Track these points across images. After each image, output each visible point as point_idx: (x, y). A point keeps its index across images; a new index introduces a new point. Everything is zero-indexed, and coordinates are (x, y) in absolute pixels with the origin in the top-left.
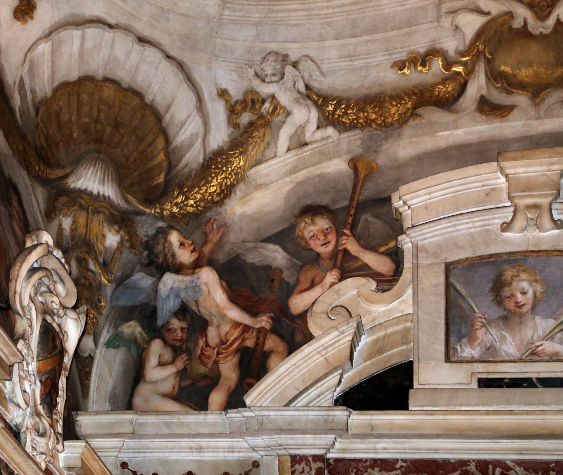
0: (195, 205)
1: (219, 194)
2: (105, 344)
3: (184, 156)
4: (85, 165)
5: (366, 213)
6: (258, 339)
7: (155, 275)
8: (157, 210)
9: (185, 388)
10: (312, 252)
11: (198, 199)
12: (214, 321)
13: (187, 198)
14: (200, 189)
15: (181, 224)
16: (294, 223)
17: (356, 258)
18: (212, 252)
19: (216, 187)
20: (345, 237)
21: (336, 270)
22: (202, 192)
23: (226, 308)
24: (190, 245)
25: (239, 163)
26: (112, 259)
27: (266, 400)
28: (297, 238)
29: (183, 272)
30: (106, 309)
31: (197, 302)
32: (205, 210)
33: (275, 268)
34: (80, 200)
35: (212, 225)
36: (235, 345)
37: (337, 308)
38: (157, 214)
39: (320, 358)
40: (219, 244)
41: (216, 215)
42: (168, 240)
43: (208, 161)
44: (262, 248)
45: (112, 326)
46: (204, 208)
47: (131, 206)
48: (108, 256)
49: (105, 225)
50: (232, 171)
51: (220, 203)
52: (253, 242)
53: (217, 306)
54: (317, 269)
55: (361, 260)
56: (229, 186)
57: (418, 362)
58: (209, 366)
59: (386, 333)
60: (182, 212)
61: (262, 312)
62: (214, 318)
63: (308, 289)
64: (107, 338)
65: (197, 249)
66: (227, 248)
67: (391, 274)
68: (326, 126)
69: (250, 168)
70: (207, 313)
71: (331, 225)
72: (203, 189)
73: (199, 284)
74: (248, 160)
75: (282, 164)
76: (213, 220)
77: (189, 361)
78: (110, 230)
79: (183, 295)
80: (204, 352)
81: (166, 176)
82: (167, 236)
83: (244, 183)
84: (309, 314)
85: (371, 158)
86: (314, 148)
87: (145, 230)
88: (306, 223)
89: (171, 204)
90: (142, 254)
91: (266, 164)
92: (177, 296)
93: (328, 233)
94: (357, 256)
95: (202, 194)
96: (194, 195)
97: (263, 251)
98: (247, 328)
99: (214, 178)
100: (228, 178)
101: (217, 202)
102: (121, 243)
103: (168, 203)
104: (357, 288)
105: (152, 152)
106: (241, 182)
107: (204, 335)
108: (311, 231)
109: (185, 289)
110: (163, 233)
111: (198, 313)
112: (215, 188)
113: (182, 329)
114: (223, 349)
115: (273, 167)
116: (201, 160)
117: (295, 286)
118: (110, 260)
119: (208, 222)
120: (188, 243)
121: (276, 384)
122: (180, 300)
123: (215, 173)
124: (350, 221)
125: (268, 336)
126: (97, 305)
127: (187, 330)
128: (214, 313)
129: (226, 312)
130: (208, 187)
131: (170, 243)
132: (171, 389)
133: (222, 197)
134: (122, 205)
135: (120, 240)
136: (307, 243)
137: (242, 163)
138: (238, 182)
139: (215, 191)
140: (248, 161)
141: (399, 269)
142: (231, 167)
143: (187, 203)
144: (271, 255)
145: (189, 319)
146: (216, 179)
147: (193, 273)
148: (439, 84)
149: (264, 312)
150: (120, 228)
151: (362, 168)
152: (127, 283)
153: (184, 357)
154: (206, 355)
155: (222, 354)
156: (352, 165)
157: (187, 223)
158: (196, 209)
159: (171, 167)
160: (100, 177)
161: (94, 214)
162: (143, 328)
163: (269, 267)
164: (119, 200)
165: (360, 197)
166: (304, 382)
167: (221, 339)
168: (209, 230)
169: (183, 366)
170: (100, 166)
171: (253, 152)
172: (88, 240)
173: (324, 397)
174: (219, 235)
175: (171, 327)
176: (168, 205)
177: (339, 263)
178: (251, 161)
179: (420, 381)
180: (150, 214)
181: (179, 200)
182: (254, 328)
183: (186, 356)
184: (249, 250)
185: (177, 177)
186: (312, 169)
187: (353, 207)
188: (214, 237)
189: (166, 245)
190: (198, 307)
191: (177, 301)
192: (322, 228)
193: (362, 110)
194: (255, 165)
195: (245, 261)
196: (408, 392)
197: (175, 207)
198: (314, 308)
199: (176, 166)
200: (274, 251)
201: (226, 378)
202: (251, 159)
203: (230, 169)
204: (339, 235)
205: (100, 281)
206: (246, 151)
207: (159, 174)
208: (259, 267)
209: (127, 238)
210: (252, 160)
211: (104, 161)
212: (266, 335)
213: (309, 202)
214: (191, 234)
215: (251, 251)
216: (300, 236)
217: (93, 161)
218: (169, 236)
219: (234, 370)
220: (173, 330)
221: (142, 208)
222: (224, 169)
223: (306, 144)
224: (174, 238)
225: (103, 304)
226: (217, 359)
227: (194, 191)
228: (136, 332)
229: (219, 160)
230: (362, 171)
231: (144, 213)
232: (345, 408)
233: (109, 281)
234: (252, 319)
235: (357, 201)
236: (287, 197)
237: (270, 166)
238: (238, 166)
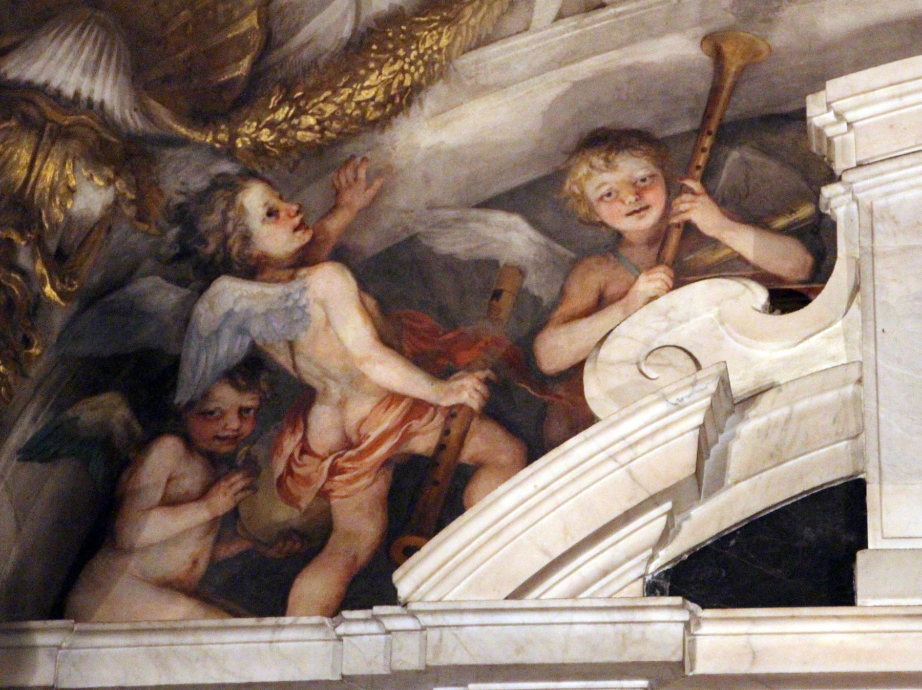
0: (317, 128)
1: (380, 106)
2: (18, 452)
3: (307, 21)
4: (57, 30)
5: (741, 144)
6: (446, 432)
7: (191, 281)
8: (222, 136)
9: (227, 560)
10: (603, 229)
11: (327, 115)
12: (333, 391)
14: (335, 92)
15: (277, 166)
16: (562, 167)
17: (715, 243)
18: (348, 230)
19: (375, 89)
20: (686, 197)
21: (662, 268)
22: (338, 100)
23: (368, 358)
24: (292, 214)
25: (438, 41)
26: (82, 245)
27: (458, 584)
28: (567, 199)
29: (265, 276)
30: (41, 364)
31: (291, 345)
32: (341, 137)
33: (505, 265)
34: (24, 107)
35: (356, 171)
36: (382, 451)
37: (664, 352)
38: (217, 145)
39: (613, 471)
40: (368, 212)
41: (369, 150)
42: (238, 203)
43: (363, 34)
44: (478, 221)
45: (48, 407)
46: (339, 133)
47: (155, 124)
48: (73, 237)
49: (80, 165)
50: (420, 56)
51: (383, 123)
52: (454, 207)
53: (346, 354)
54: (615, 268)
55: (727, 247)
56: (407, 88)
57: (880, 484)
58: (303, 505)
59: (792, 411)
60: (283, 141)
61: (464, 369)
62: (331, 383)
63: (587, 313)
64: (29, 437)
65: (311, 221)
66: (386, 222)
67: (802, 276)
69: (464, 53)
70: (317, 372)
71: (653, 170)
72: (342, 95)
73: (303, 302)
74: (461, 33)
75: (540, 44)
76: (359, 159)
77: (248, 492)
78: (91, 178)
79: (256, 328)
80: (297, 470)
81: (255, 64)
82: (236, 193)
83: (444, 83)
84: (588, 367)
85: (755, 33)
86: (621, 14)
87: (181, 179)
88: (592, 167)
89: (259, 123)
90: (163, 232)
91: (503, 43)
92: (242, 330)
93: (645, 189)
94: (717, 236)
95: (341, 105)
96: (317, 107)
97: (480, 228)
98: (418, 407)
99: (372, 70)
100: (408, 71)
101: (375, 121)
102: (114, 208)
103: (252, 121)
104: (718, 304)
105: (229, 12)
106: (438, 80)
107: (301, 425)
108: (604, 184)
109: (265, 314)
111: (292, 371)
112: (372, 93)
113: (242, 411)
114: (349, 459)
115: (519, 52)
116: (346, 31)
117: (555, 305)
118: (76, 245)
119: (346, 163)
120: (286, 210)
121: (490, 539)
122: (247, 341)
123: (376, 60)
124: (701, 160)
125: (474, 424)
126: (16, 353)
127: (255, 418)
128: (333, 371)
129: (367, 368)
130: (355, 90)
131: (243, 210)
132: (184, 569)
133: (388, 110)
134: (130, 121)
135: (112, 200)
136: (591, 209)
137: (444, 42)
138: (431, 80)
139: (373, 99)
140: (459, 39)
141: (823, 268)
142: (417, 49)
143: (300, 123)
144: (499, 236)
145: (264, 386)
146: (377, 72)
147: (292, 278)
149: (469, 368)
150: (117, 174)
151: (734, 53)
152: (112, 301)
153: (238, 481)
154: (299, 475)
155: (342, 471)
156: (708, 47)
157: (291, 165)
158: (319, 135)
159: (269, 43)
160: (86, 62)
161: (56, 138)
162: (136, 411)
163: (493, 263)
164: (127, 112)
165: (728, 112)
166: (566, 530)
167: (344, 432)
168: (347, 182)
169: (232, 505)
170: (94, 33)
172: (26, 197)
173: (619, 577)
174: (371, 192)
175: (212, 406)
176: (249, 127)
177: (670, 252)
178: (466, 35)
179: (885, 531)
180: (200, 145)
181: (280, 115)
182: (436, 407)
183: (241, 479)
184: (443, 225)
185: (281, 66)
186: (614, 55)
187: (710, 133)
188: (357, 198)
189: (231, 214)
190: (293, 356)
191: (239, 342)
192: (630, 177)
194: (477, 46)
195: (430, 250)
196: (853, 559)
197: (266, 131)
198: (604, 351)
199: (281, 44)
200: (508, 228)
201: (348, 534)
202: (467, 32)
203: (414, 53)
204: (673, 190)
205: (38, 296)
206: (459, 14)
207: (238, 59)
208: (466, 264)
209: (131, 196)
210: (470, 34)
211: (104, 25)
212: (469, 424)
213: (602, 122)
214: (299, 190)
215: (449, 227)
216: (574, 193)
217: (79, 21)
218: (240, 195)
219: (371, 515)
220: (217, 414)
221: (183, 130)
222: (401, 52)
225: (36, 351)
226: (328, 486)
227: (319, 96)
228: (113, 421)
229: (390, 34)
230: (733, 60)
231: (184, 142)
232: (678, 600)
233: (61, 294)
234: (434, 386)
235: (721, 120)
236: (549, 114)
237: (511, 49)
238: (435, 48)
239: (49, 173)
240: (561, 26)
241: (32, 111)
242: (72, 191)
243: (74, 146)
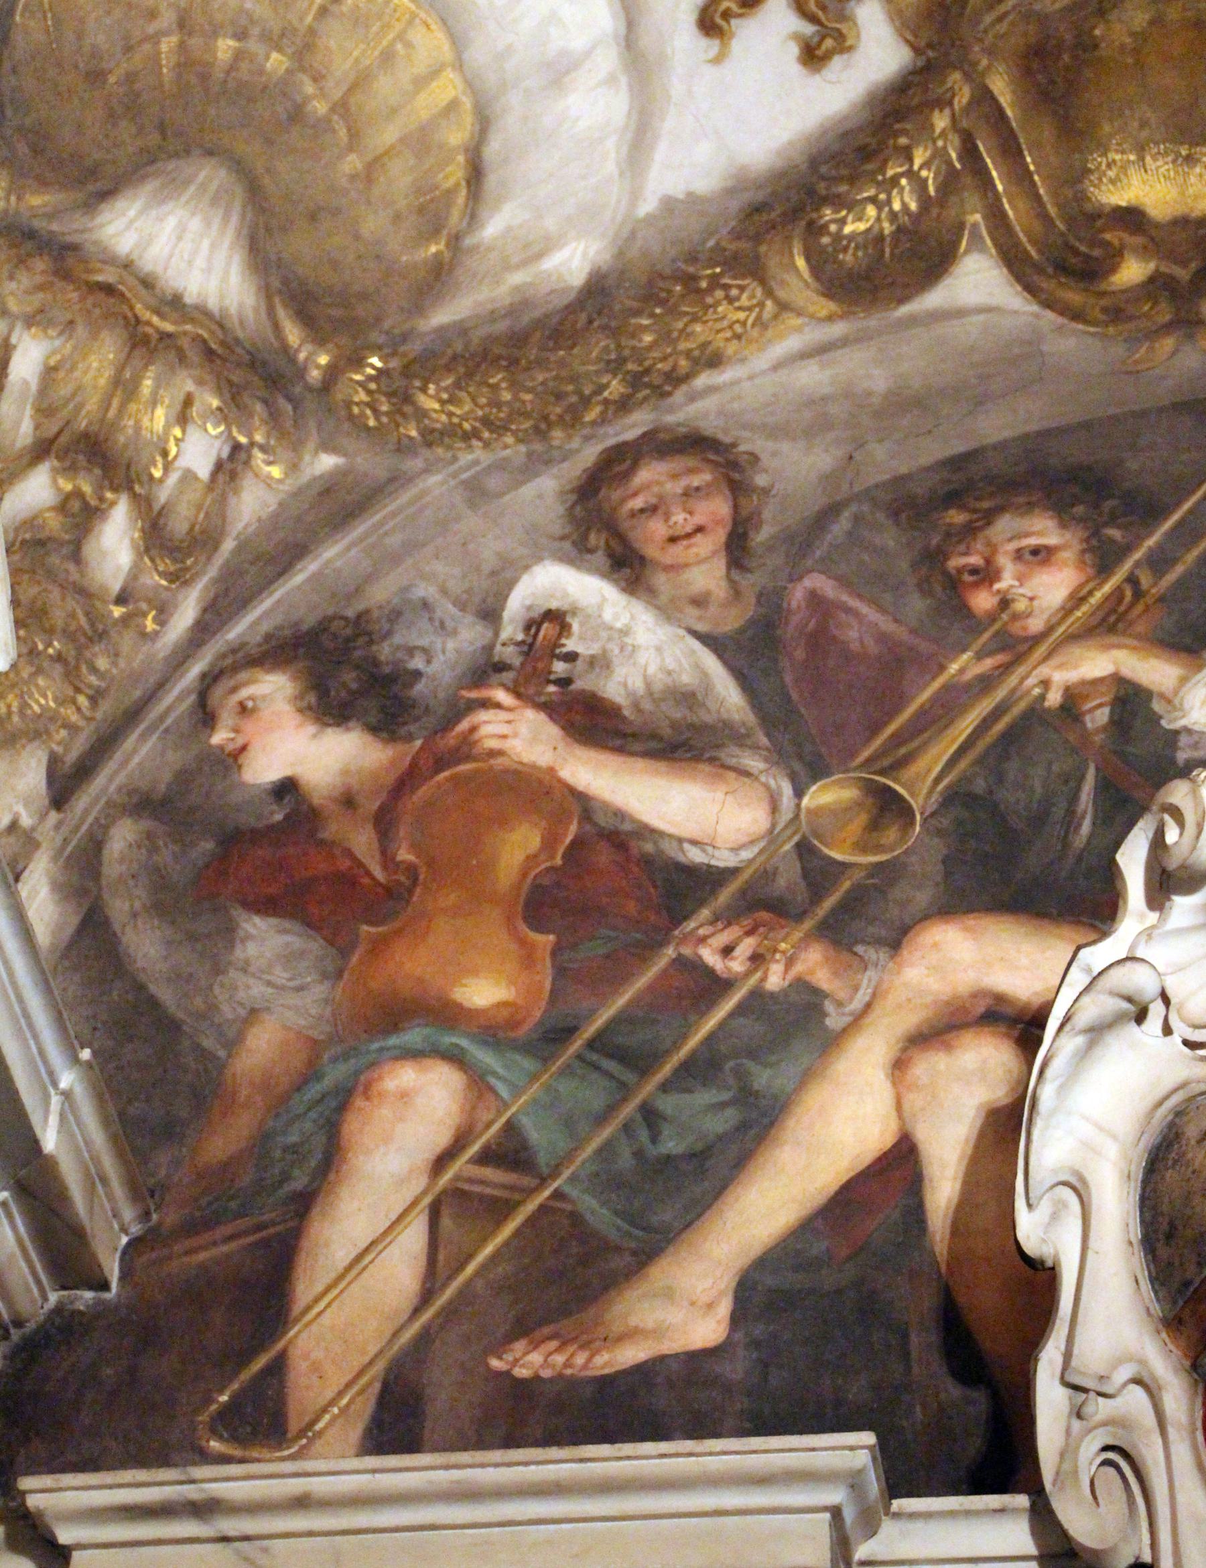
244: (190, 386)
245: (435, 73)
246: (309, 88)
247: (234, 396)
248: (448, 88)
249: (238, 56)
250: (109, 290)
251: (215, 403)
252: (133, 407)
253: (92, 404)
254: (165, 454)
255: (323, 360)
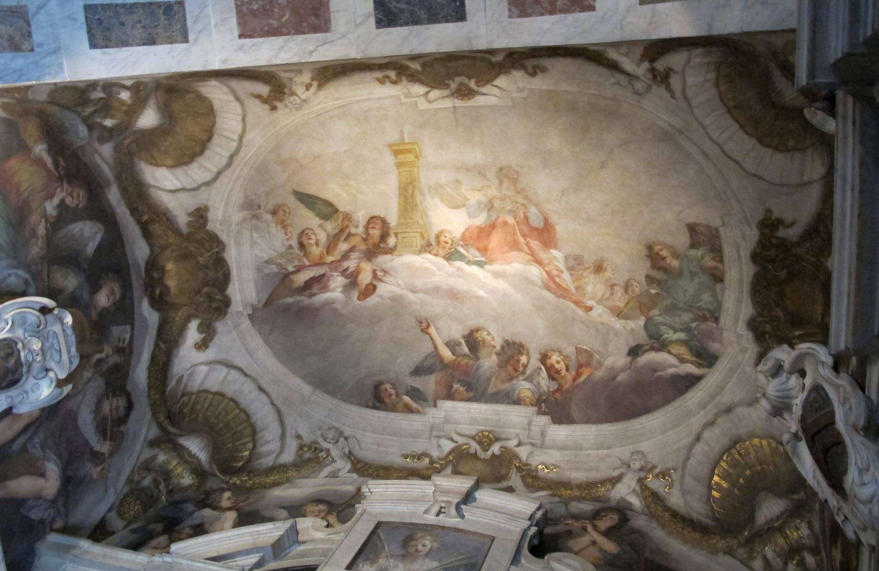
8: (227, 479)
13: (250, 479)
14: (261, 478)
22: (261, 480)
50: (286, 476)
68: (353, 473)
95: (261, 481)
110: (222, 490)
137: (295, 475)
138: (286, 482)
148: (425, 469)
171: (303, 472)
181: (244, 478)
193: (377, 471)
223: (337, 477)
224: (227, 494)
233: (166, 500)
239: (179, 470)
240: (324, 479)
241: (182, 454)
242: (182, 477)
243: (188, 466)
244: (793, 524)
245: (761, 443)
246: (755, 468)
247: (801, 517)
248: (764, 442)
249: (743, 479)
250: (769, 528)
251: (799, 521)
252: (790, 538)
253: (785, 546)
254: (802, 537)
255: (803, 494)
